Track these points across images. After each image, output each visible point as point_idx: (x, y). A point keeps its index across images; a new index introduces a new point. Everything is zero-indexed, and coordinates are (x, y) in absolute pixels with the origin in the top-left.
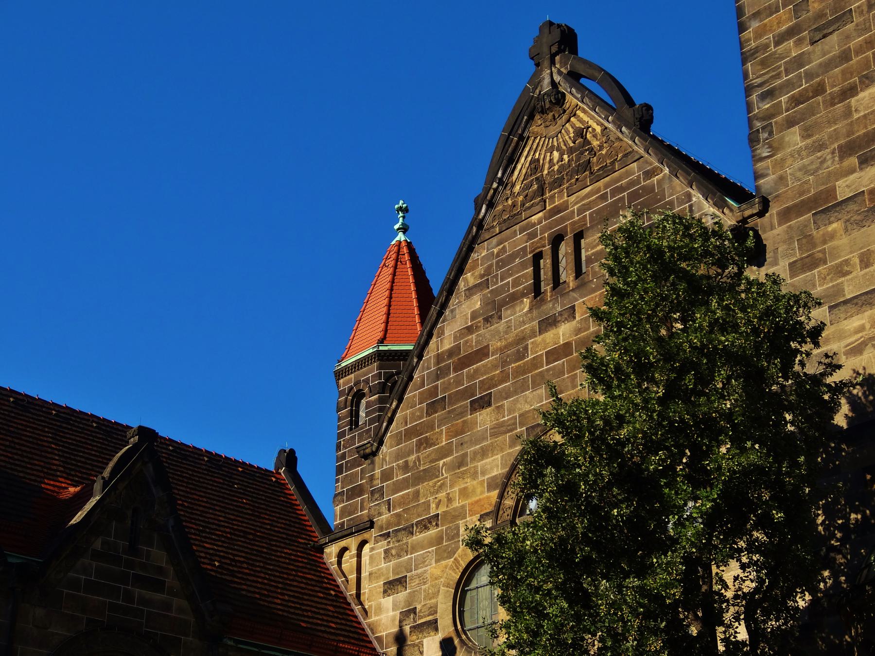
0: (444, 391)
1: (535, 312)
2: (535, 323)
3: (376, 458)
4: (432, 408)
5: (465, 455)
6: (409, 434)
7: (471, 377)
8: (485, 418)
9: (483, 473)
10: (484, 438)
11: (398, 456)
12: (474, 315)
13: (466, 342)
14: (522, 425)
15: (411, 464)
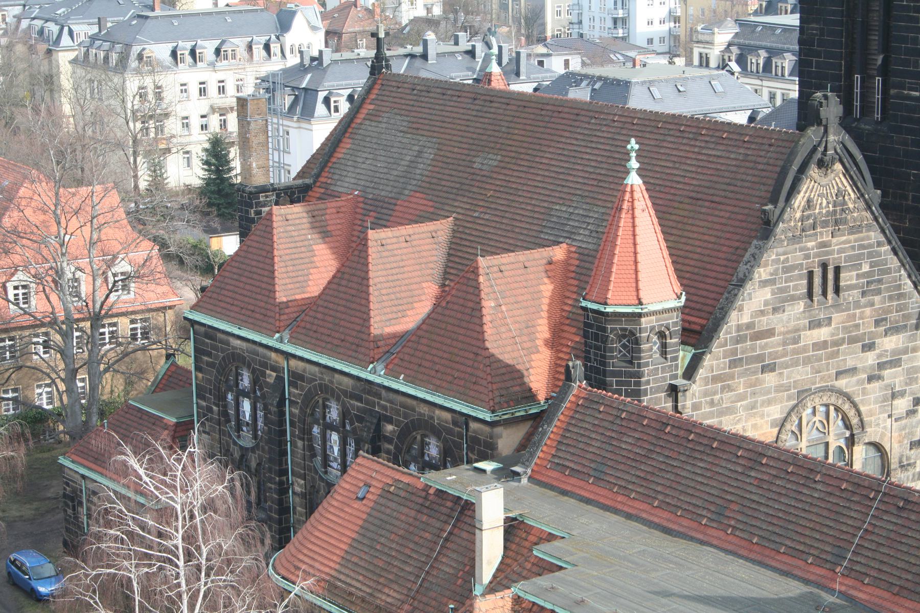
0: (742, 353)
1: (807, 314)
2: (807, 321)
3: (687, 393)
4: (734, 364)
5: (756, 402)
6: (715, 379)
7: (762, 348)
8: (770, 379)
9: (768, 416)
10: (769, 392)
11: (706, 394)
12: (766, 303)
13: (760, 321)
14: (795, 388)
15: (716, 402)
